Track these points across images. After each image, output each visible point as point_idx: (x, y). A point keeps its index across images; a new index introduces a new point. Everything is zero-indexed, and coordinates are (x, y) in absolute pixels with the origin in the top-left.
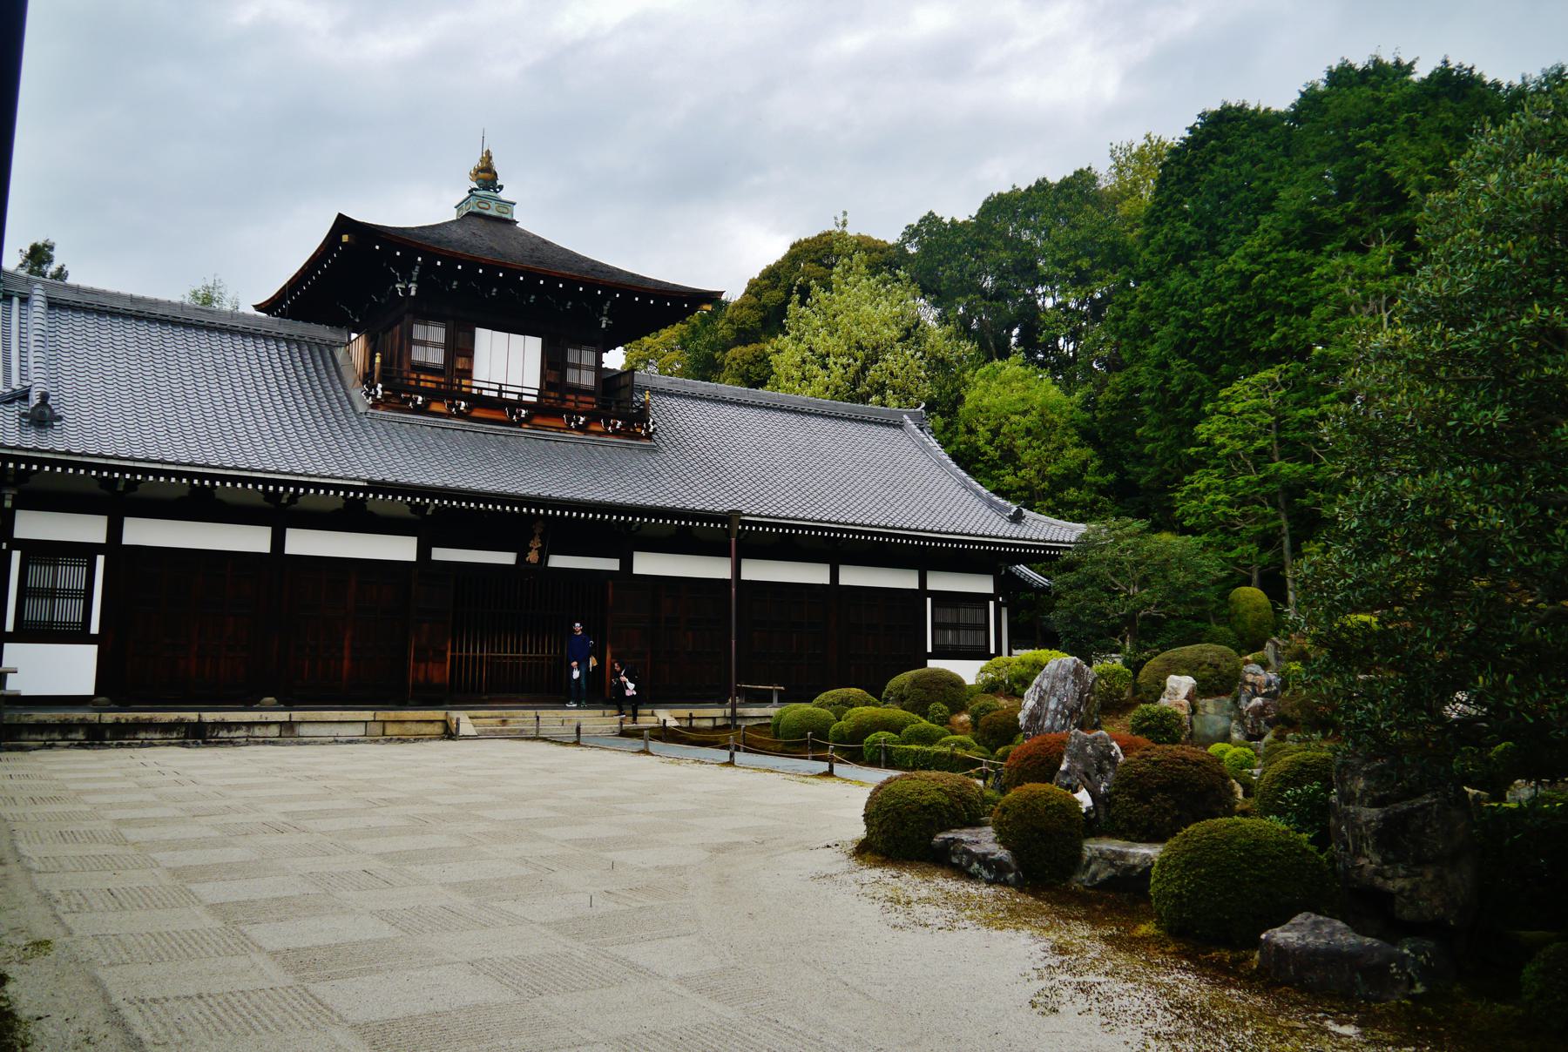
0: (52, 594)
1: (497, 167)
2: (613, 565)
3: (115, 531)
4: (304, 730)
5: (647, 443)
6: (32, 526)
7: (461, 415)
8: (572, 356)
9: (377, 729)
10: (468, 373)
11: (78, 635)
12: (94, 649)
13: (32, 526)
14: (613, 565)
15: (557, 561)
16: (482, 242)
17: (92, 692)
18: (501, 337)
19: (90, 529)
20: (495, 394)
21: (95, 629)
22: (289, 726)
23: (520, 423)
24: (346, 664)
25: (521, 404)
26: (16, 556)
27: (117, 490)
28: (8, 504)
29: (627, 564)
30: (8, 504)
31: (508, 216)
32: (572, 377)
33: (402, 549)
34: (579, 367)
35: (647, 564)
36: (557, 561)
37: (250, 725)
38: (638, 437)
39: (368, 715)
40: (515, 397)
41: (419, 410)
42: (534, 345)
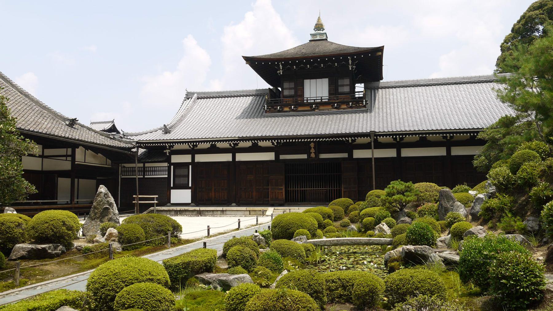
0: (180, 176)
1: (323, 21)
2: (345, 155)
3: (193, 158)
4: (227, 213)
5: (364, 109)
6: (175, 159)
7: (293, 111)
8: (340, 82)
9: (248, 213)
11: (186, 187)
12: (189, 191)
13: (175, 159)
14: (345, 155)
15: (323, 156)
16: (321, 49)
17: (189, 201)
18: (313, 81)
19: (187, 159)
20: (305, 101)
21: (190, 185)
22: (223, 211)
23: (314, 110)
24: (254, 194)
25: (314, 103)
26: (172, 167)
27: (193, 147)
28: (168, 154)
29: (351, 154)
30: (168, 154)
31: (324, 38)
32: (341, 90)
33: (269, 156)
34: (343, 86)
35: (358, 154)
36: (323, 156)
37: (213, 211)
38: (360, 107)
39: (244, 208)
40: (313, 101)
41: (279, 111)
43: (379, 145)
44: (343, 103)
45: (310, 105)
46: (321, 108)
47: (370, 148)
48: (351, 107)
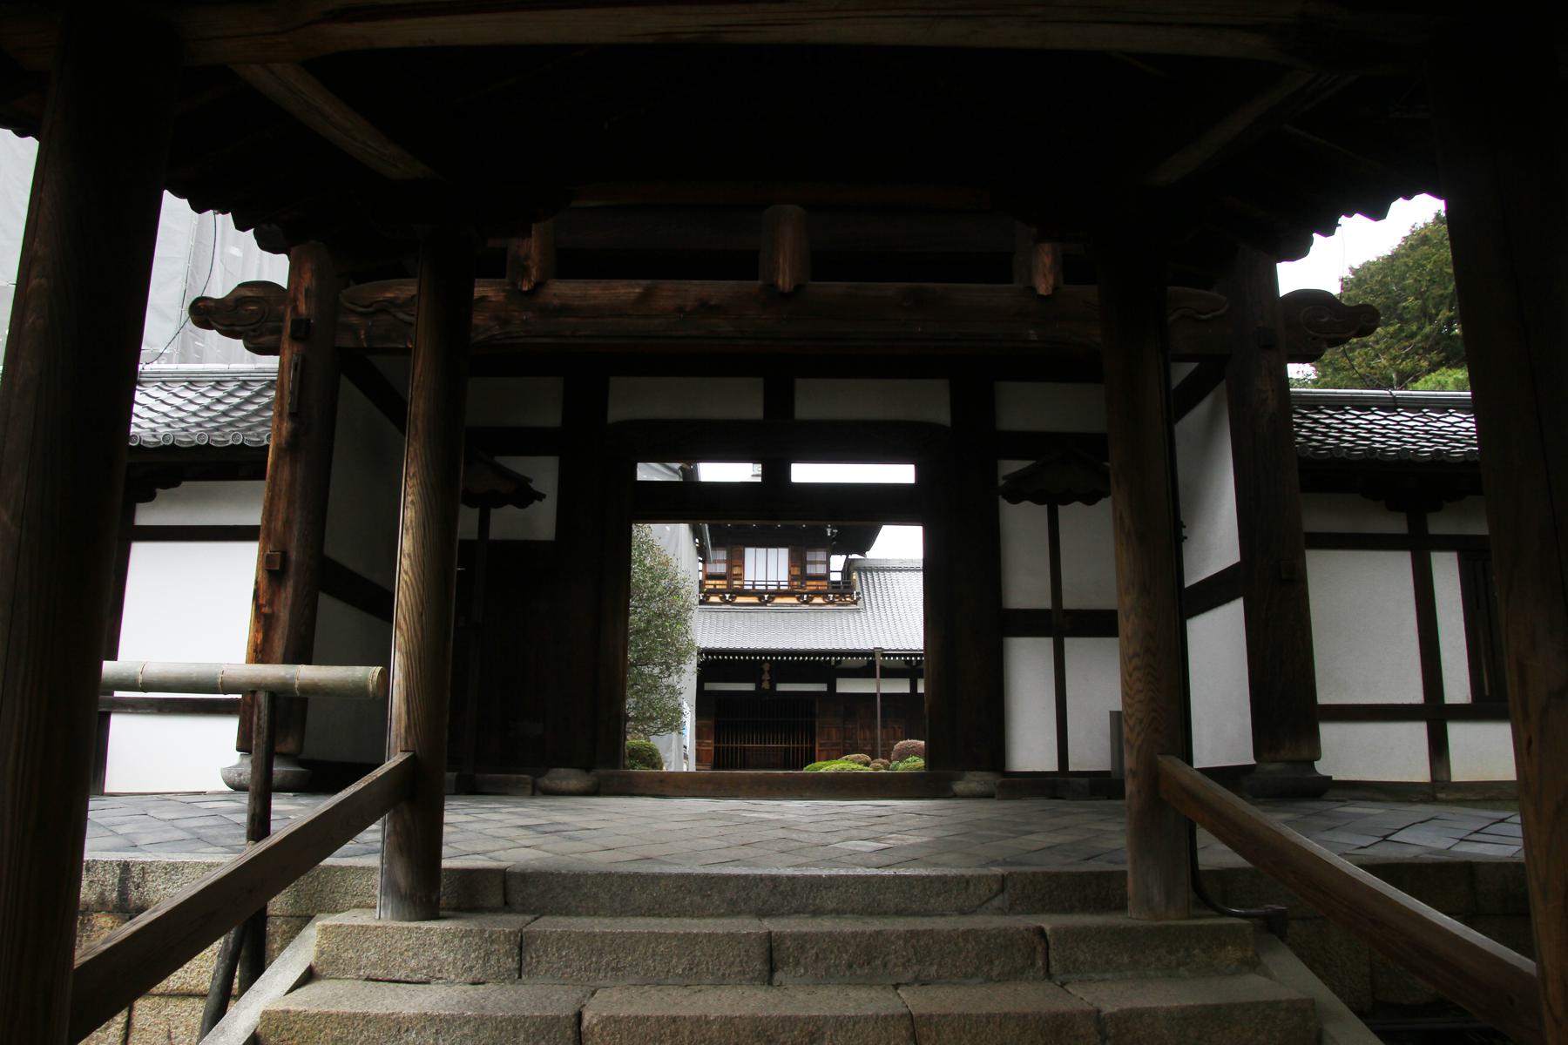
2: (822, 687)
7: (727, 602)
8: (810, 556)
10: (740, 577)
14: (822, 687)
15: (782, 687)
18: (761, 551)
23: (765, 604)
25: (766, 592)
29: (832, 686)
32: (811, 570)
34: (815, 563)
35: (846, 686)
36: (782, 687)
42: (784, 553)
43: (889, 673)
44: (817, 593)
45: (759, 594)
46: (778, 600)
47: (874, 676)
48: (832, 603)
